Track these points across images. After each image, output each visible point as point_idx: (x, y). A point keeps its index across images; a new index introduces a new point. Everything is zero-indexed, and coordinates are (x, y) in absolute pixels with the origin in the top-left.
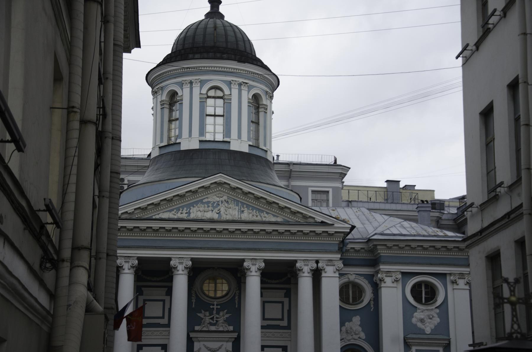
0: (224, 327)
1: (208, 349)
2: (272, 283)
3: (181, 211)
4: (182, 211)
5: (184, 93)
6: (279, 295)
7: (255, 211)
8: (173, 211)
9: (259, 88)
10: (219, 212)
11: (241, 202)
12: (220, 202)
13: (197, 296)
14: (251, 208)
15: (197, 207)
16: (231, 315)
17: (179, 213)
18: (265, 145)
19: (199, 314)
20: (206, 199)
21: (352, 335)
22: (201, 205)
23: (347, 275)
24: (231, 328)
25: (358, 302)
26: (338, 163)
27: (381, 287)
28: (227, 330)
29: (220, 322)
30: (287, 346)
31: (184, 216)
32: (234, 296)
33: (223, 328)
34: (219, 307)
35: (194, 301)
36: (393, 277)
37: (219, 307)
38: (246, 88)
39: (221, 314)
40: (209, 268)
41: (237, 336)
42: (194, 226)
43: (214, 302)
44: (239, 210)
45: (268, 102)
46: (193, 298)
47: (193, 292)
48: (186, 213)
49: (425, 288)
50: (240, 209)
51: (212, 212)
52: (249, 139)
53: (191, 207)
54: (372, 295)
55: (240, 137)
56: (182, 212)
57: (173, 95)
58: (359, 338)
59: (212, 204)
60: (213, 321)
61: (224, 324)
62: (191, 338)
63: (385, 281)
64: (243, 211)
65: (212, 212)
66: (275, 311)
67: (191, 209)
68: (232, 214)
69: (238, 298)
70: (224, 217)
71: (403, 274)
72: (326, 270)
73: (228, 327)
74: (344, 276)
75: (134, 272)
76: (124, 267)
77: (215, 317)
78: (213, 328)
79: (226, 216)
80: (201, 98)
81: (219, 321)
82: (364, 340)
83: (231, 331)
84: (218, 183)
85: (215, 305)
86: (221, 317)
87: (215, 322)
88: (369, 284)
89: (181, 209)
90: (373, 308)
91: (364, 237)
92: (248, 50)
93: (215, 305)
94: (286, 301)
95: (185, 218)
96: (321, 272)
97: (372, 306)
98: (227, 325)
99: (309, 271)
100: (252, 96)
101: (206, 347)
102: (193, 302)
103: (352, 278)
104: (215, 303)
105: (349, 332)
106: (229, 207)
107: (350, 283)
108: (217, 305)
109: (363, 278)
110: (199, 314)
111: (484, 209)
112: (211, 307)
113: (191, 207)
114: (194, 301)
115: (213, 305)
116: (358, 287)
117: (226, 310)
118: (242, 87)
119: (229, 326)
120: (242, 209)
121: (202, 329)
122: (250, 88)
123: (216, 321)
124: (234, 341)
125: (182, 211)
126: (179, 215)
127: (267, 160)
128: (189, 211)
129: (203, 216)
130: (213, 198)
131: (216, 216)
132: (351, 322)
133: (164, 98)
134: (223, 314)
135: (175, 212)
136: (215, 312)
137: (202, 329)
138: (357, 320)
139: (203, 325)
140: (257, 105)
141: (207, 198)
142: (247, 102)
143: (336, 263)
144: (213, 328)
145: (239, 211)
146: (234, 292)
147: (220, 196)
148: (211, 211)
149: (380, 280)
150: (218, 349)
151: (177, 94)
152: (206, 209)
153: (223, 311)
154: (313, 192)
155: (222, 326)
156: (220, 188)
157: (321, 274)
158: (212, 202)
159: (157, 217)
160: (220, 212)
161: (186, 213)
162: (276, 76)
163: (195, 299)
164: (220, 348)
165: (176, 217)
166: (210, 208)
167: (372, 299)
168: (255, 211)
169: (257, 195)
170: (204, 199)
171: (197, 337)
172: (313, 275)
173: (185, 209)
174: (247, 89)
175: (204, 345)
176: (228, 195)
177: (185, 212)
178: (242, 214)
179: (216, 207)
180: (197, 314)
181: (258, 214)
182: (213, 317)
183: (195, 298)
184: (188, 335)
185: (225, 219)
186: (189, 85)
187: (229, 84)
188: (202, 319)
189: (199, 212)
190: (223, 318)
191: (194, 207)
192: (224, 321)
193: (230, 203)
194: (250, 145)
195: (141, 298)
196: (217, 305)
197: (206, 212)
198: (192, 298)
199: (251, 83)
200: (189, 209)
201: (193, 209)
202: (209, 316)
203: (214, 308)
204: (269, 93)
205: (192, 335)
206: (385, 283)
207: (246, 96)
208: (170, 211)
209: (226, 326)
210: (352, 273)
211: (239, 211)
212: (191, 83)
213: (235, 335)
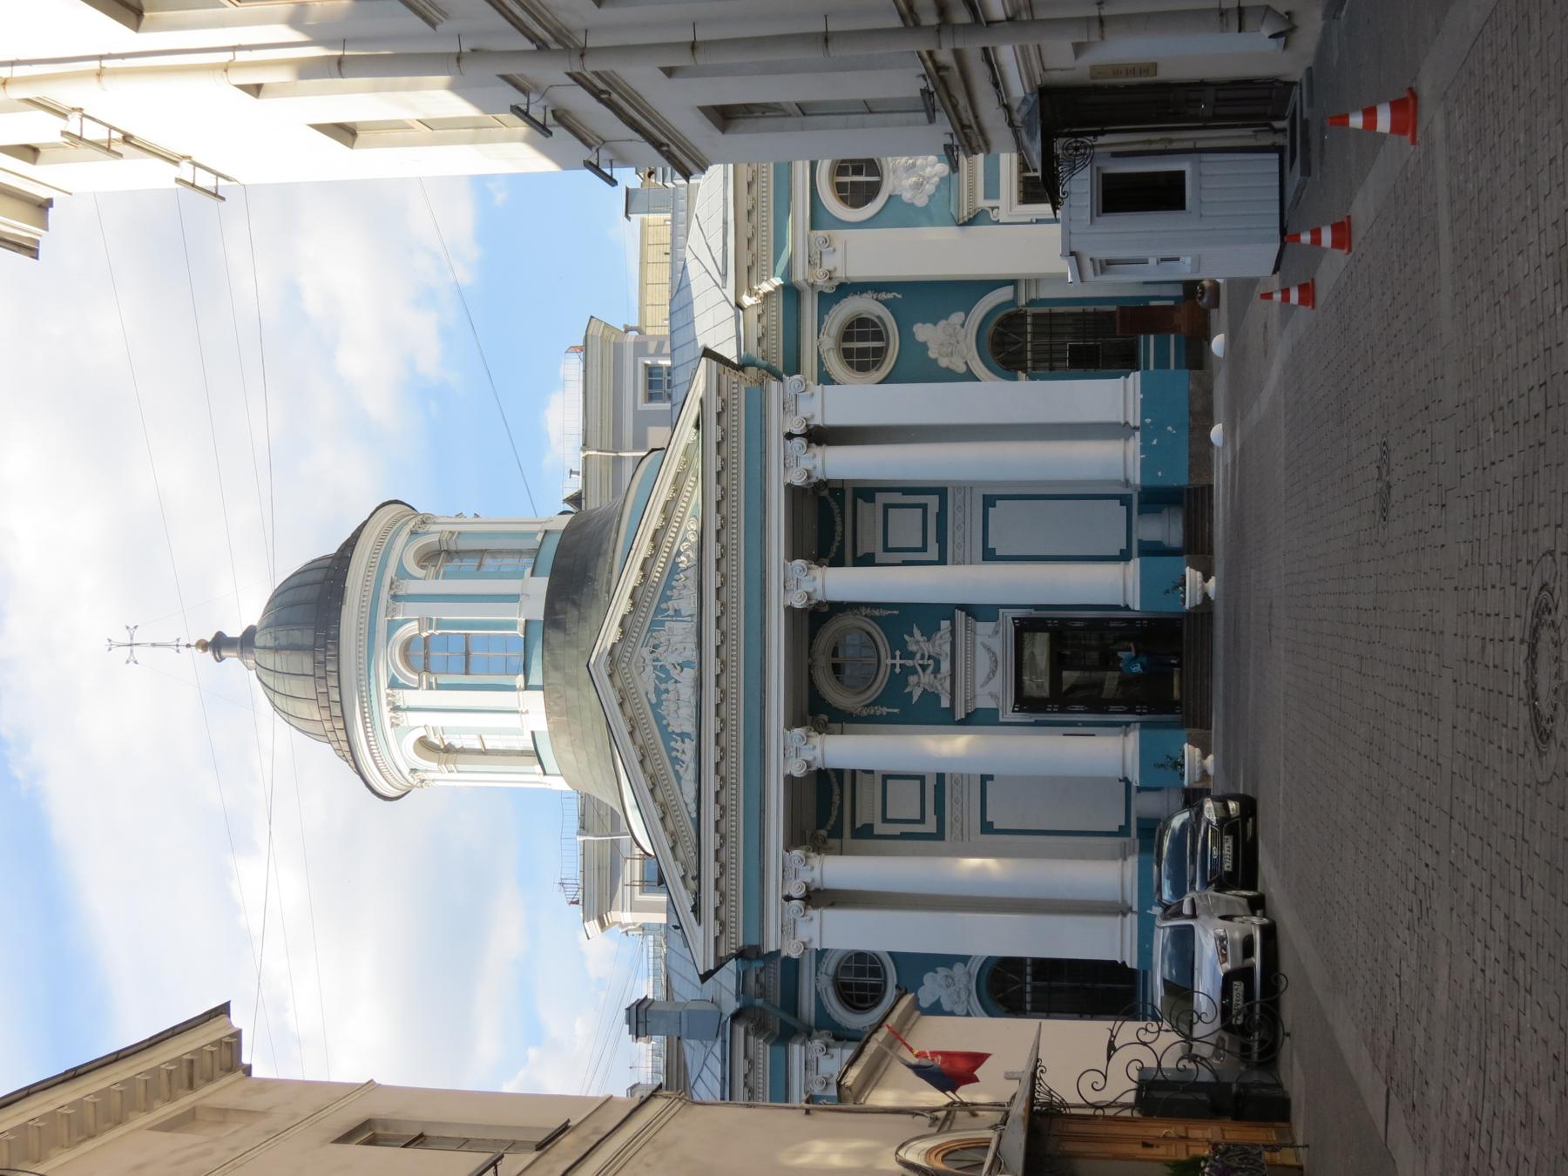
0: (941, 641)
2: (843, 532)
3: (679, 755)
4: (678, 751)
5: (418, 723)
6: (870, 515)
7: (674, 583)
8: (678, 771)
9: (405, 552)
10: (678, 667)
11: (655, 614)
12: (654, 663)
13: (874, 704)
14: (669, 593)
15: (668, 718)
17: (683, 757)
18: (535, 534)
19: (915, 698)
20: (649, 696)
21: (958, 343)
22: (663, 708)
23: (821, 351)
24: (945, 624)
25: (882, 329)
26: (581, 343)
27: (846, 277)
28: (948, 635)
29: (931, 650)
30: (984, 496)
31: (689, 746)
33: (945, 642)
34: (898, 653)
35: (885, 710)
36: (823, 250)
37: (898, 653)
38: (403, 583)
39: (913, 648)
40: (810, 675)
41: (963, 610)
42: (711, 725)
43: (887, 665)
44: (672, 621)
45: (433, 528)
46: (878, 713)
47: (865, 713)
48: (683, 742)
49: (847, 175)
50: (672, 616)
51: (680, 682)
52: (518, 575)
53: (670, 729)
54: (865, 295)
55: (514, 598)
56: (680, 751)
57: (424, 745)
58: (963, 325)
59: (661, 683)
60: (929, 665)
61: (937, 643)
62: (968, 715)
63: (831, 268)
64: (676, 611)
65: (680, 682)
66: (906, 529)
67: (673, 732)
68: (682, 635)
70: (690, 653)
71: (814, 225)
72: (808, 415)
74: (824, 360)
75: (818, 857)
76: (809, 880)
77: (921, 662)
78: (945, 666)
79: (687, 650)
80: (430, 687)
81: (929, 652)
82: (966, 317)
83: (951, 625)
84: (611, 669)
85: (894, 662)
86: (921, 648)
87: (931, 662)
88: (841, 302)
89: (674, 754)
90: (895, 294)
91: (732, 312)
92: (319, 575)
93: (894, 662)
94: (881, 498)
95: (694, 743)
96: (811, 427)
97: (890, 296)
98: (942, 632)
99: (810, 454)
100: (422, 567)
101: (987, 683)
102: (888, 712)
103: (829, 342)
104: (889, 661)
105: (950, 349)
106: (667, 643)
107: (840, 345)
108: (894, 657)
109: (826, 317)
110: (915, 698)
111: (598, 137)
112: (898, 670)
113: (670, 729)
114: (885, 710)
115: (894, 666)
116: (849, 327)
117: (906, 636)
118: (400, 593)
119: (939, 629)
120: (671, 612)
121: (946, 691)
122: (402, 573)
123: (928, 659)
124: (973, 617)
125: (678, 751)
126: (689, 756)
127: (567, 532)
128: (677, 734)
129: (689, 702)
130: (646, 682)
131: (689, 674)
132: (929, 344)
133: (434, 765)
135: (682, 766)
136: (910, 661)
137: (946, 691)
138: (923, 332)
139: (939, 688)
140: (443, 554)
141: (647, 694)
142: (434, 580)
143: (790, 392)
144: (945, 666)
145: (676, 621)
146: (864, 618)
147: (641, 664)
148: (678, 685)
149: (830, 278)
151: (425, 737)
152: (671, 696)
154: (651, 398)
155: (940, 645)
156: (624, 665)
157: (818, 427)
158: (657, 682)
159: (693, 807)
160: (678, 665)
161: (683, 742)
162: (378, 509)
164: (989, 650)
165: (692, 765)
166: (670, 685)
167: (875, 297)
168: (674, 583)
169: (637, 579)
170: (649, 700)
171: (966, 701)
172: (819, 444)
173: (673, 744)
174: (405, 582)
175: (982, 686)
176: (639, 646)
177: (679, 743)
178: (683, 613)
179: (667, 672)
181: (682, 575)
182: (920, 665)
184: (962, 722)
185: (695, 653)
186: (400, 713)
187: (393, 626)
188: (925, 690)
189: (680, 712)
190: (922, 644)
191: (668, 725)
192: (929, 640)
193: (656, 642)
194: (532, 575)
195: (880, 828)
196: (894, 657)
197: (679, 697)
199: (390, 572)
200: (674, 736)
201: (673, 726)
202: (919, 677)
203: (900, 665)
204: (414, 527)
205: (960, 714)
206: (835, 269)
207: (425, 583)
208: (679, 778)
209: (941, 638)
210: (816, 344)
211: (674, 619)
212: (396, 709)
213: (960, 616)
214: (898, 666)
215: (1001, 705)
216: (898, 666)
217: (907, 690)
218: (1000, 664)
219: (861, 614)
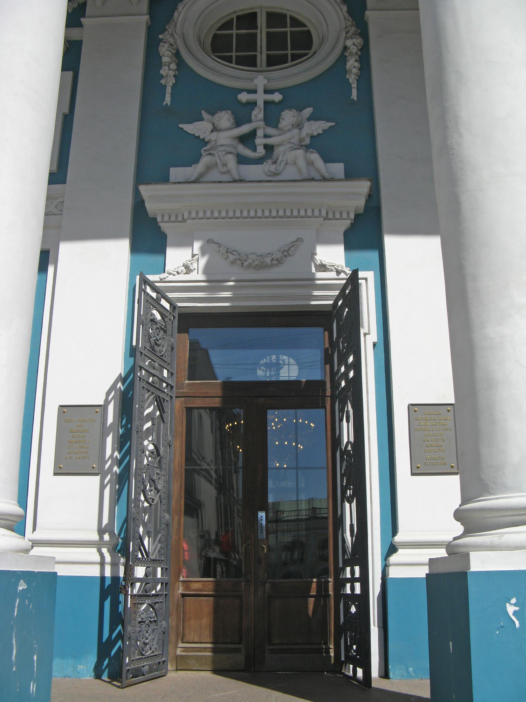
0: (302, 163)
1: (231, 257)
16: (331, 127)
19: (189, 128)
32: (342, 59)
34: (277, 97)
60: (254, 149)
69: (357, 64)
73: (319, 162)
77: (260, 133)
81: (280, 144)
93: (261, 90)
102: (165, 87)
110: (189, 128)
114: (169, 82)
117: (308, 111)
123: (266, 147)
134: (294, 120)
136: (261, 115)
150: (275, 256)
153: (300, 109)
163: (172, 73)
180: (181, 126)
182: (253, 134)
183: (170, 69)
188: (205, 143)
190: (296, 131)
198: (162, 72)
214: (251, 97)
215: (171, 278)
216: (251, 97)
217: (205, 115)
218: (256, 296)
219: (346, 38)
